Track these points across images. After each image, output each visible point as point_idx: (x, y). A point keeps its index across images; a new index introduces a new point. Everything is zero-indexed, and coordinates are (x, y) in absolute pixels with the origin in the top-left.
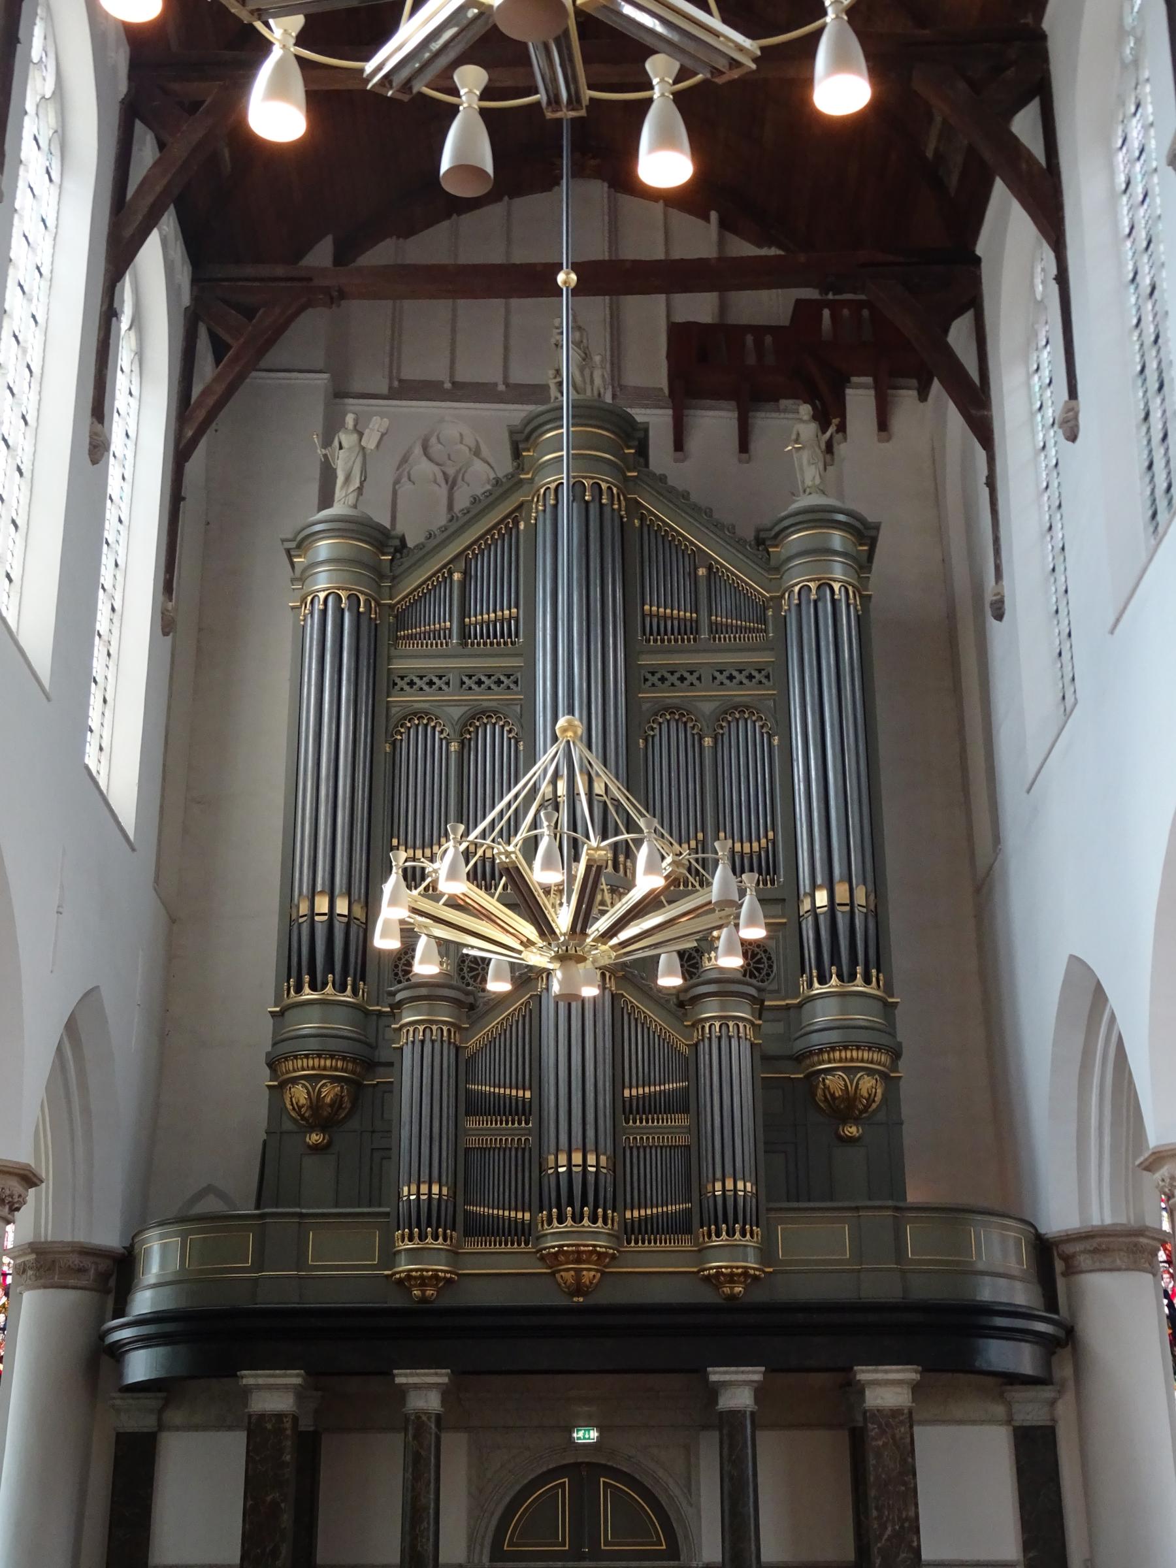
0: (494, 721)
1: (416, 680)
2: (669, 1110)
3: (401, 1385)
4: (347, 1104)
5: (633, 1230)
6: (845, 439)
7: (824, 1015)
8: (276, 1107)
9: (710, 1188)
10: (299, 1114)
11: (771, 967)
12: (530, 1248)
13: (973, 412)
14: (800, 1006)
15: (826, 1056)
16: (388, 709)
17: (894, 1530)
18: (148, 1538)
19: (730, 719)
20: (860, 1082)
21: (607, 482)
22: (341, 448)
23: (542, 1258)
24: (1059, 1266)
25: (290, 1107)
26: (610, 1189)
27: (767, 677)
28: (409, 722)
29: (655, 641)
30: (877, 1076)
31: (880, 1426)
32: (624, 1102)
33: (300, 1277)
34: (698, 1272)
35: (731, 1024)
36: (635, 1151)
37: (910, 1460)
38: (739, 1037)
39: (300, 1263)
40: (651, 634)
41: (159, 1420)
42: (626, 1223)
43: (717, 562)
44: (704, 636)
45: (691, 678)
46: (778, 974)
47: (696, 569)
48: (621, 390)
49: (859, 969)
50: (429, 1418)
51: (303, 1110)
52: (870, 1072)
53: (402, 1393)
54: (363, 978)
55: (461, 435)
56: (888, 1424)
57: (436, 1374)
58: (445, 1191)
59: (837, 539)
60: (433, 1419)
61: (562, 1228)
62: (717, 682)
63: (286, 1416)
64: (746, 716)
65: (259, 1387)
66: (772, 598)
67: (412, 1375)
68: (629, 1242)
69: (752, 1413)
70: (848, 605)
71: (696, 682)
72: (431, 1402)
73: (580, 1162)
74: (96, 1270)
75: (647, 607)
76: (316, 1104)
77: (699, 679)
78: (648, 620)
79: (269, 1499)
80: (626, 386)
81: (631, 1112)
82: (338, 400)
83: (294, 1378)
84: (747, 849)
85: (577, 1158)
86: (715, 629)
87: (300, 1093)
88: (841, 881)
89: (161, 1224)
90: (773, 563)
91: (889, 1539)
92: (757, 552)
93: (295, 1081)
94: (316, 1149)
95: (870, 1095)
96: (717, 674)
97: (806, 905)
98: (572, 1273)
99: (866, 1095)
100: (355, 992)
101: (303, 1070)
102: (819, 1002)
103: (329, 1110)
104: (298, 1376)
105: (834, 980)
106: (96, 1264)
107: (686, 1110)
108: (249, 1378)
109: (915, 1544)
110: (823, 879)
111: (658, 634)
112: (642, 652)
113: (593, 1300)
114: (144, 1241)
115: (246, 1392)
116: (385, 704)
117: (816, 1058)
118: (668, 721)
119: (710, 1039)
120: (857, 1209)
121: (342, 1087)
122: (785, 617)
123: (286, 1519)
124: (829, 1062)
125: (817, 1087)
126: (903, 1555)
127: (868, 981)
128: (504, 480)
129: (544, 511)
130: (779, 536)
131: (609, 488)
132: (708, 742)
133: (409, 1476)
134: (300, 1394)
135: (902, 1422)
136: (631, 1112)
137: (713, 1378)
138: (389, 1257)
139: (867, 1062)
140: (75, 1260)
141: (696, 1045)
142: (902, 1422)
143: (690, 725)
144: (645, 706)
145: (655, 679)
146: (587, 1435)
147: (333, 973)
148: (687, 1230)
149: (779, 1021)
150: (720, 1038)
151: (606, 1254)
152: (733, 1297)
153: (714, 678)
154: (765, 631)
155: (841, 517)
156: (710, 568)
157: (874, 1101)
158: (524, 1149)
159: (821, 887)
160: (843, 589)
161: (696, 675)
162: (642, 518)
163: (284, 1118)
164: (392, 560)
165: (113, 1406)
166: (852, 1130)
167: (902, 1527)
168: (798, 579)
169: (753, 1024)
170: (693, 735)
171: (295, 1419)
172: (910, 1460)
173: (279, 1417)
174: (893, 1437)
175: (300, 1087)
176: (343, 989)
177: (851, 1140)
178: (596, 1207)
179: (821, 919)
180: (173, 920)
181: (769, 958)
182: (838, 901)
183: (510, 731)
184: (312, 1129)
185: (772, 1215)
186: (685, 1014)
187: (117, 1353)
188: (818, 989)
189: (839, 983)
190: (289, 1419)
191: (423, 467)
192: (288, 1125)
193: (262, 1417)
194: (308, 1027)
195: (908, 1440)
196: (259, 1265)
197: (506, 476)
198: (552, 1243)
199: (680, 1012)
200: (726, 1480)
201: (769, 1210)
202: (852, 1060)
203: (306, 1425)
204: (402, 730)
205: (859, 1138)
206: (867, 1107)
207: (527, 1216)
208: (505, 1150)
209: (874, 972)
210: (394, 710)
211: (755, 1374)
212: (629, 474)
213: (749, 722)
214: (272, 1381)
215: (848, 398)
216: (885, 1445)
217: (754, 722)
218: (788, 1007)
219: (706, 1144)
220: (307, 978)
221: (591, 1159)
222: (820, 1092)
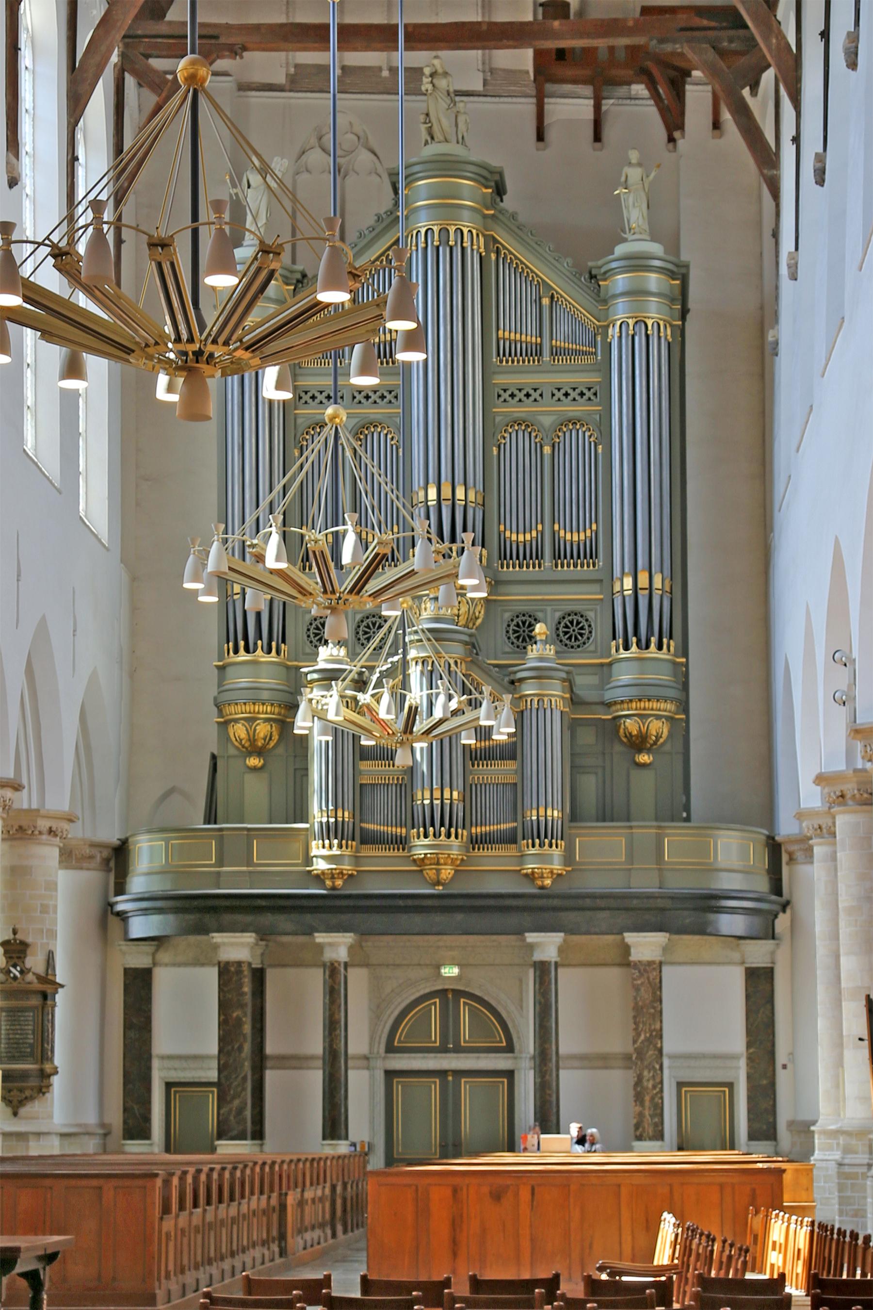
0: (379, 430)
1: (317, 394)
2: (502, 758)
3: (320, 944)
4: (276, 737)
5: (476, 841)
6: (683, 137)
7: (624, 676)
9: (529, 813)
10: (241, 743)
11: (590, 632)
12: (405, 854)
13: (765, 171)
14: (610, 664)
15: (625, 706)
16: (295, 420)
17: (645, 1037)
18: (151, 1037)
19: (565, 429)
20: (651, 725)
21: (468, 227)
22: (249, 187)
23: (414, 861)
24: (785, 858)
25: (234, 739)
26: (461, 814)
27: (595, 394)
28: (313, 429)
29: (507, 362)
30: (663, 720)
31: (639, 972)
32: (471, 752)
33: (250, 872)
34: (520, 871)
35: (546, 699)
36: (479, 786)
37: (658, 993)
38: (552, 709)
39: (250, 863)
40: (504, 355)
41: (154, 958)
42: (472, 837)
43: (557, 293)
44: (546, 357)
45: (535, 395)
46: (595, 640)
47: (540, 298)
48: (492, 73)
49: (653, 640)
50: (339, 965)
51: (243, 742)
52: (658, 717)
54: (284, 641)
55: (350, 123)
56: (645, 970)
57: (343, 937)
58: (346, 814)
59: (653, 281)
60: (342, 965)
61: (426, 842)
62: (555, 398)
63: (243, 962)
64: (578, 427)
65: (224, 944)
66: (601, 326)
67: (327, 937)
68: (474, 849)
69: (556, 963)
70: (659, 338)
71: (539, 398)
72: (342, 954)
73: (439, 797)
74: (101, 856)
75: (501, 332)
76: (252, 740)
77: (541, 395)
78: (502, 343)
79: (235, 1015)
80: (496, 69)
81: (476, 759)
82: (242, 93)
83: (249, 938)
84: (575, 538)
86: (555, 352)
87: (239, 731)
88: (643, 570)
89: (149, 831)
90: (602, 294)
91: (642, 1042)
92: (589, 284)
93: (236, 721)
94: (254, 769)
95: (658, 734)
96: (555, 392)
97: (617, 588)
98: (434, 871)
99: (655, 733)
100: (278, 652)
101: (242, 713)
102: (623, 664)
103: (263, 741)
104: (251, 937)
105: (634, 648)
106: (101, 852)
107: (514, 758)
108: (218, 938)
109: (659, 1045)
110: (630, 569)
111: (510, 355)
112: (494, 373)
114: (137, 842)
115: (216, 947)
116: (292, 417)
117: (618, 707)
118: (517, 431)
119: (531, 709)
120: (631, 827)
121: (271, 726)
122: (610, 343)
123: (247, 1028)
124: (628, 710)
125: (620, 726)
126: (651, 1053)
127: (660, 647)
128: (384, 216)
129: (417, 250)
130: (606, 275)
131: (470, 231)
132: (547, 450)
133: (327, 1001)
134: (253, 947)
135: (654, 969)
136: (476, 759)
137: (529, 940)
138: (308, 860)
139: (656, 710)
140: (87, 851)
141: (522, 712)
142: (654, 969)
143: (533, 434)
144: (498, 419)
145: (506, 395)
146: (450, 971)
147: (261, 639)
149: (596, 674)
150: (538, 709)
151: (456, 859)
152: (542, 888)
153: (553, 395)
154: (595, 353)
155: (657, 263)
156: (552, 297)
157: (661, 737)
158: (401, 785)
159: (628, 574)
160: (655, 324)
161: (539, 392)
162: (498, 252)
163: (230, 746)
164: (295, 290)
165: (121, 950)
166: (644, 758)
167: (651, 1035)
168: (621, 311)
169: (563, 698)
170: (536, 443)
171: (250, 964)
172: (658, 993)
173: (239, 964)
174: (648, 978)
175: (240, 725)
176: (269, 651)
177: (644, 766)
178: (450, 826)
179: (627, 599)
180: (134, 579)
181: (590, 626)
182: (640, 586)
183: (392, 439)
184: (250, 754)
185: (573, 831)
186: (515, 689)
187: (123, 917)
188: (623, 654)
189: (638, 650)
190: (246, 965)
191: (316, 157)
192: (232, 751)
194: (244, 682)
195: (658, 980)
196: (220, 863)
197: (386, 213)
198: (419, 853)
199: (512, 687)
200: (537, 1005)
201: (570, 827)
202: (644, 709)
203: (256, 965)
204: (307, 437)
205: (650, 764)
206: (655, 743)
207: (404, 830)
208: (388, 785)
209: (665, 640)
210: (299, 421)
212: (487, 212)
213: (580, 431)
214: (233, 940)
215: (688, 95)
216: (642, 984)
217: (584, 432)
218: (602, 665)
219: (527, 783)
220: (242, 644)
222: (622, 731)
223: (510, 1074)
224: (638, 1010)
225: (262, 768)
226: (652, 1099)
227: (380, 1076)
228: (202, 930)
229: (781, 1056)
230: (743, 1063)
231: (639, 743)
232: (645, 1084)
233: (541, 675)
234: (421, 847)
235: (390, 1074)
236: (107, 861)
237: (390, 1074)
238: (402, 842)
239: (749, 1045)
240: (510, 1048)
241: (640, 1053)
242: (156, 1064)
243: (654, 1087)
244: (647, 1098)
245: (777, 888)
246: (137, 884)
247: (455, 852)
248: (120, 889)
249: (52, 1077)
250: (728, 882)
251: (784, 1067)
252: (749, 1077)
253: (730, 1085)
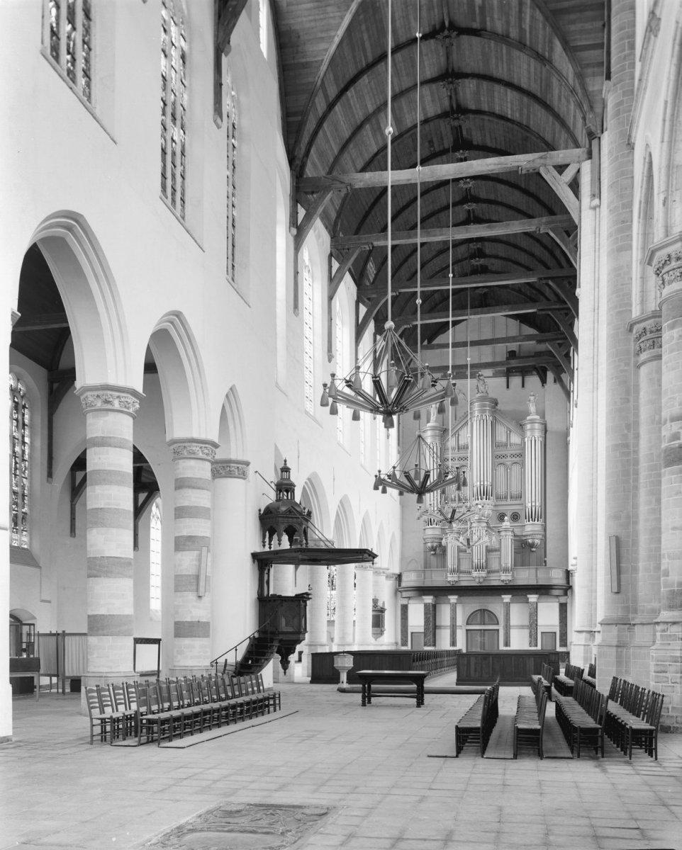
5: (489, 572)
8: (425, 547)
53: (450, 599)
76: (432, 547)
83: (431, 597)
87: (429, 545)
108: (424, 597)
115: (423, 599)
123: (431, 619)
138: (447, 578)
148: (498, 572)
166: (534, 549)
177: (533, 551)
211: (510, 596)
223: (498, 630)
224: (531, 615)
225: (435, 554)
228: (421, 595)
230: (558, 628)
231: (532, 545)
233: (506, 530)
234: (475, 574)
235: (467, 630)
236: (396, 578)
237: (467, 630)
238: (470, 573)
239: (560, 623)
240: (498, 624)
241: (531, 625)
242: (409, 628)
245: (568, 582)
246: (403, 584)
247: (484, 575)
248: (400, 585)
250: (555, 582)
252: (560, 631)
253: (555, 633)
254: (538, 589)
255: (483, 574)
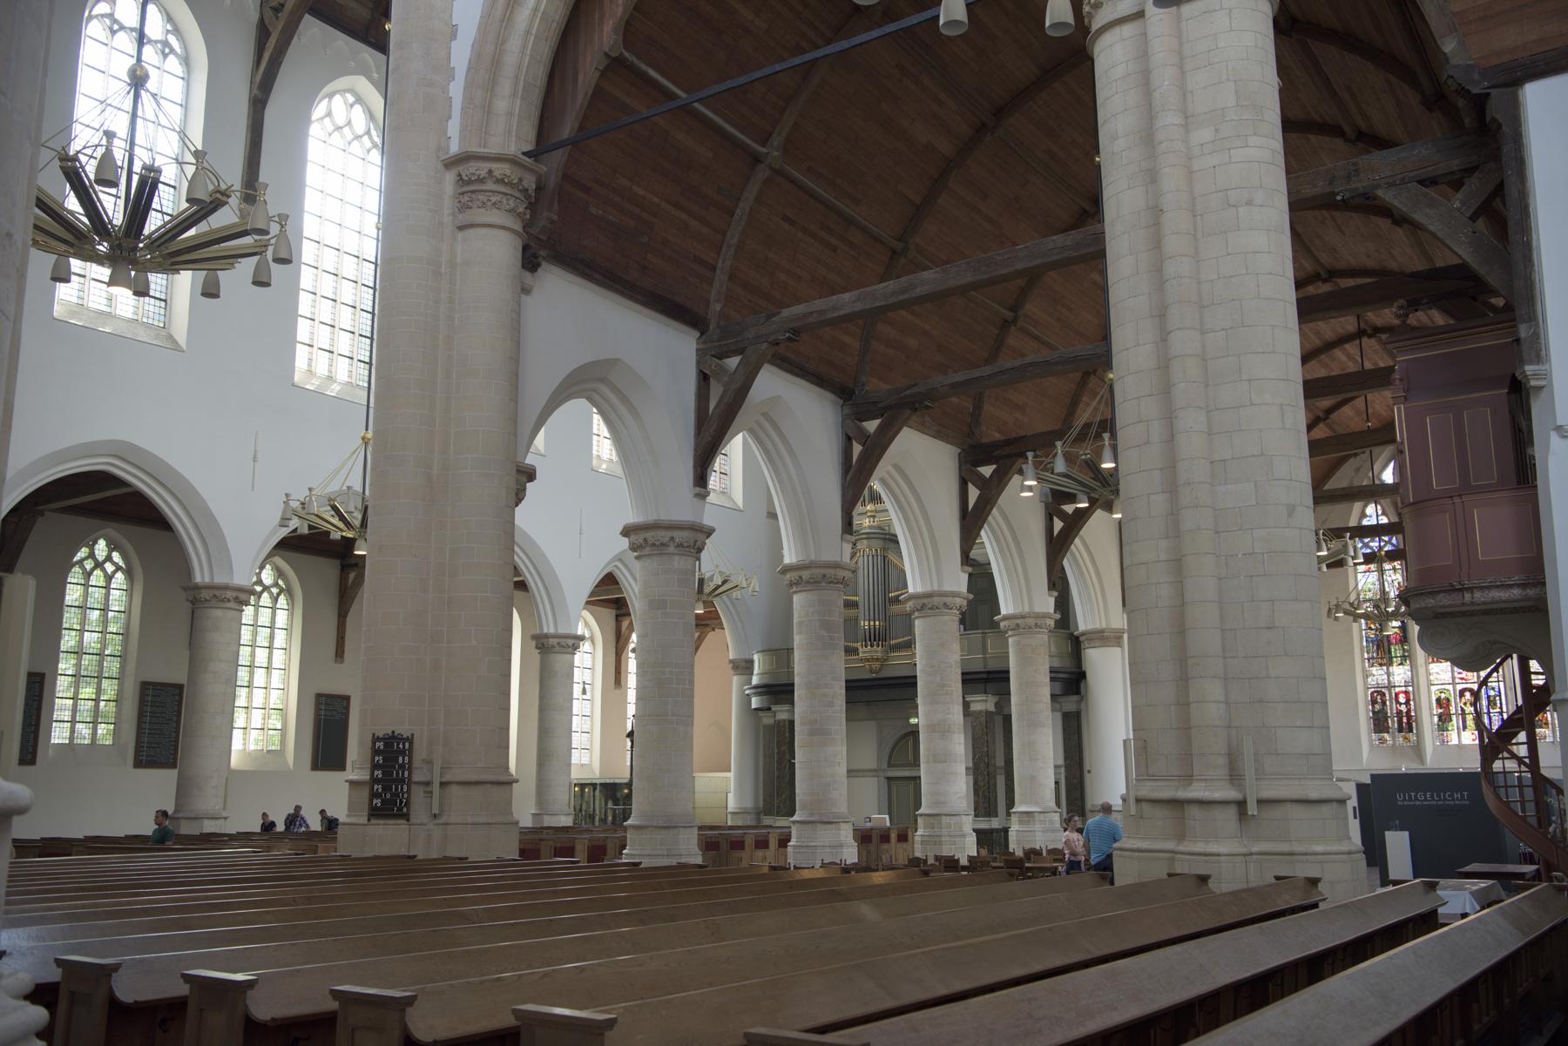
85: (872, 623)
113: (880, 676)
140: (744, 664)
173: (784, 720)
193: (779, 721)
221: (877, 623)
226: (983, 792)
227: (884, 781)
229: (1087, 767)
232: (979, 784)
235: (889, 779)
239: (1066, 759)
243: (984, 786)
244: (981, 792)
249: (514, 784)
251: (1089, 772)
252: (1067, 778)
254: (986, 681)
255: (878, 651)
